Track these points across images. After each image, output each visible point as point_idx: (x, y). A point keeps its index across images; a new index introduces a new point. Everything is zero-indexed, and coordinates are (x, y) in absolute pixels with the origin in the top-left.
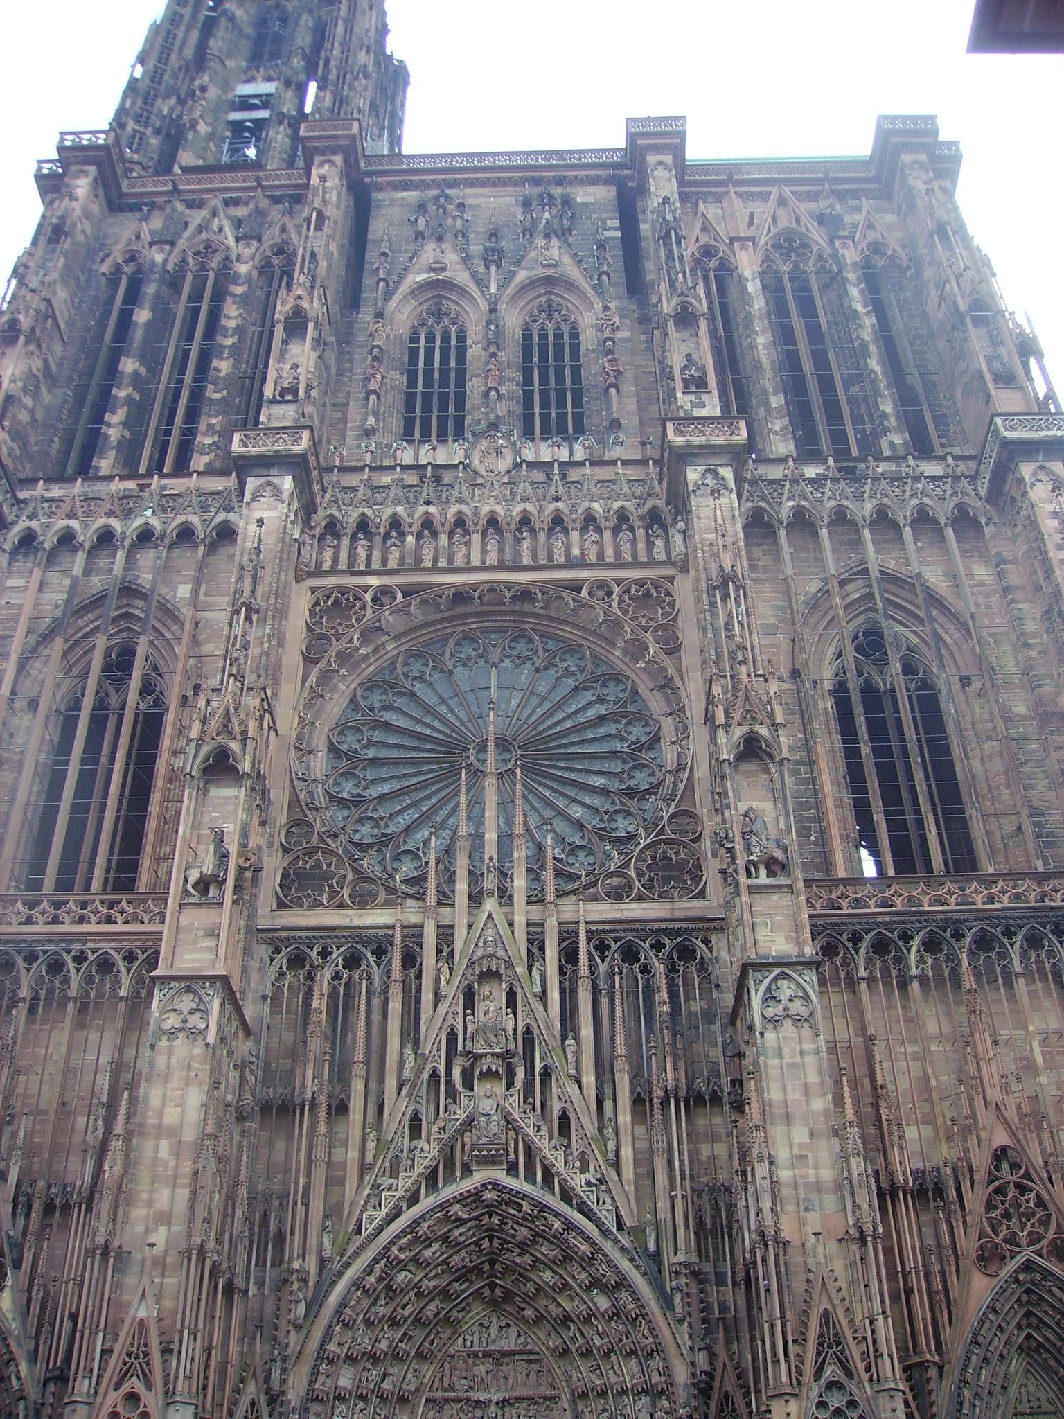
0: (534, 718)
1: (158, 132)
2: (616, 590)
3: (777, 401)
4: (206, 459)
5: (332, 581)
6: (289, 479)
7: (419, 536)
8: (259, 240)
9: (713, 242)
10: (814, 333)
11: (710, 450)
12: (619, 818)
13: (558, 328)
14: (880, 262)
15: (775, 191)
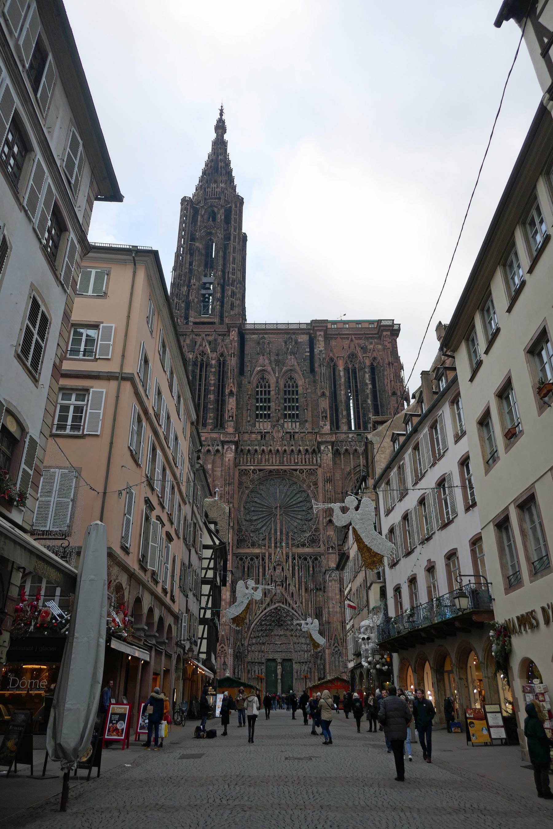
0: (287, 501)
1: (183, 301)
2: (305, 471)
3: (345, 413)
4: (210, 427)
5: (243, 468)
6: (234, 446)
7: (261, 455)
8: (217, 352)
9: (333, 357)
10: (356, 386)
11: (327, 442)
12: (304, 525)
13: (293, 385)
14: (375, 365)
15: (350, 336)
